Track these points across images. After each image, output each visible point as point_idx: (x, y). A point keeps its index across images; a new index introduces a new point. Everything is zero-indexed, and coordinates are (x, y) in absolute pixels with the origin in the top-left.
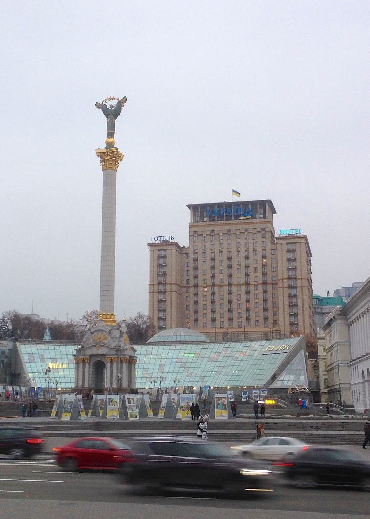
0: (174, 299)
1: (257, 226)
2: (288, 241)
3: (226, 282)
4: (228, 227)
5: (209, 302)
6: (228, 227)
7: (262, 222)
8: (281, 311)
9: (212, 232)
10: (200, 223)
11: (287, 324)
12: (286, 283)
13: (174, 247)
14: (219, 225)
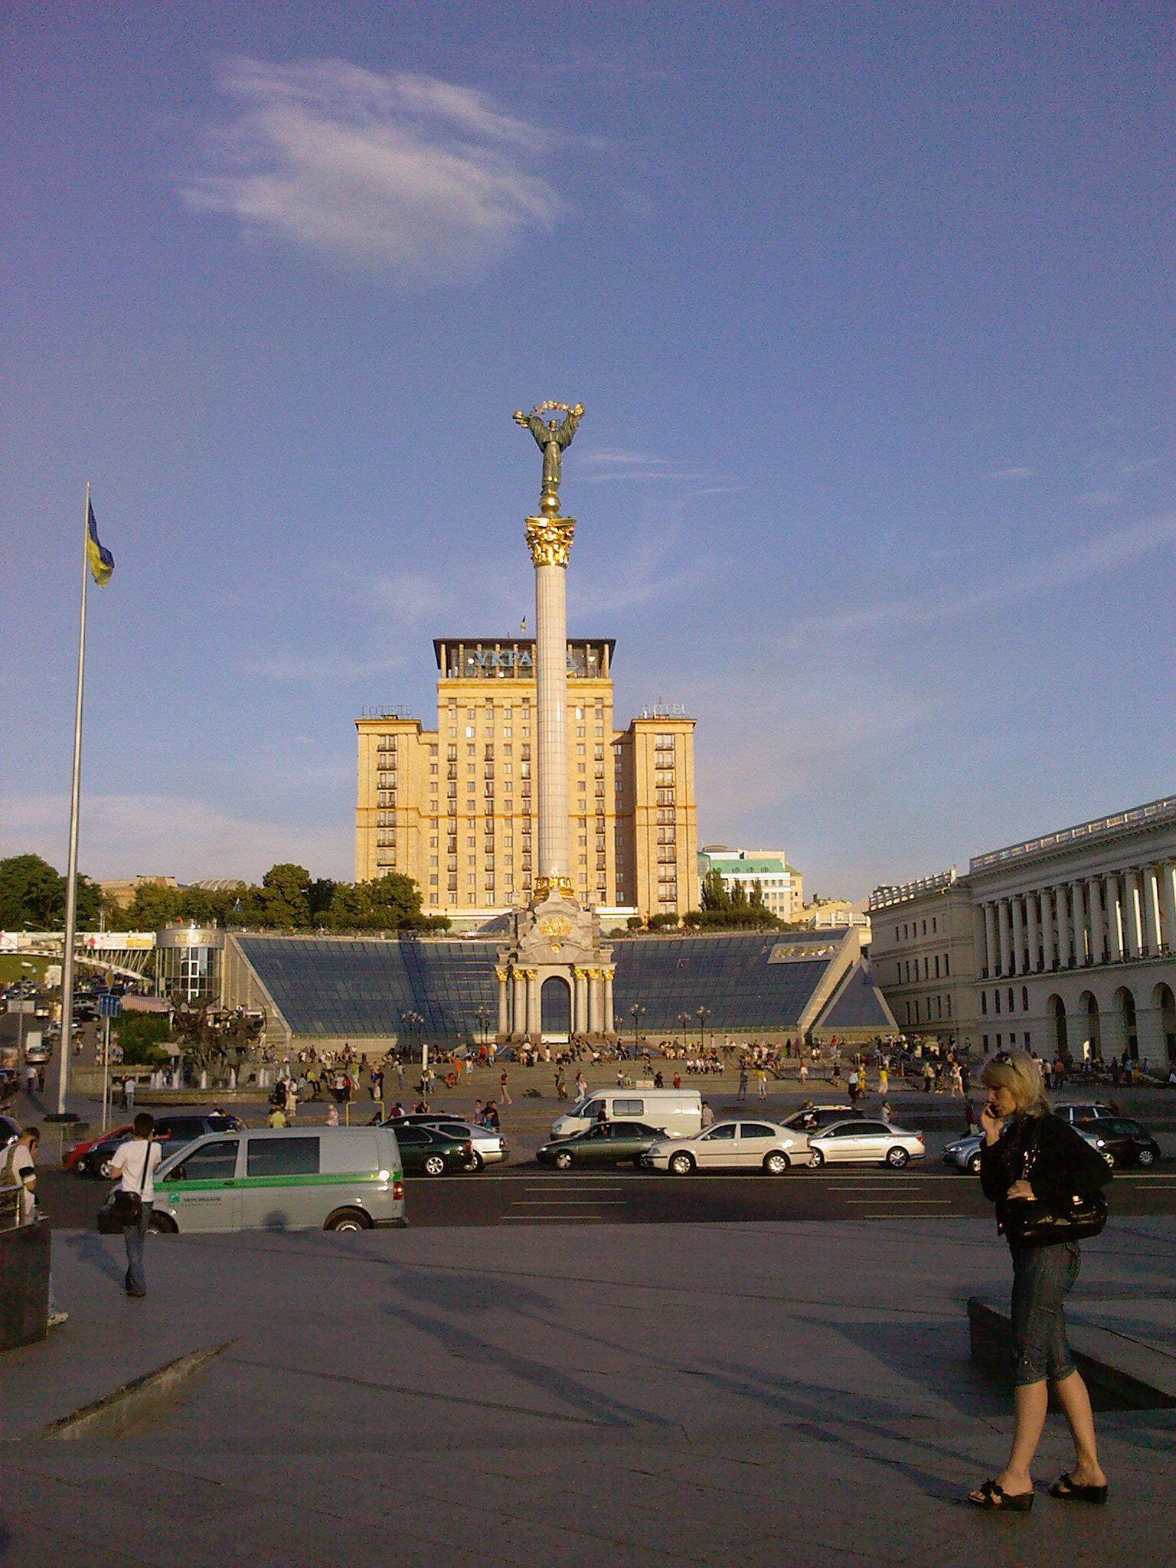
0: (413, 843)
1: (586, 692)
2: (658, 728)
3: (519, 806)
4: (523, 692)
5: (480, 851)
6: (523, 692)
7: (596, 685)
8: (641, 872)
9: (490, 700)
10: (462, 681)
11: (654, 899)
12: (656, 815)
13: (414, 729)
14: (502, 686)
